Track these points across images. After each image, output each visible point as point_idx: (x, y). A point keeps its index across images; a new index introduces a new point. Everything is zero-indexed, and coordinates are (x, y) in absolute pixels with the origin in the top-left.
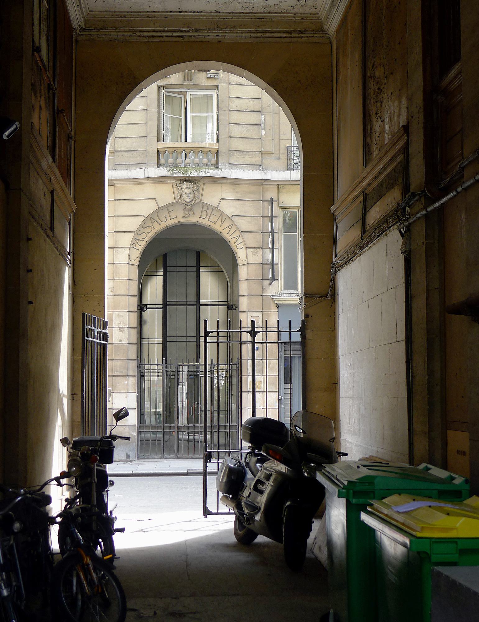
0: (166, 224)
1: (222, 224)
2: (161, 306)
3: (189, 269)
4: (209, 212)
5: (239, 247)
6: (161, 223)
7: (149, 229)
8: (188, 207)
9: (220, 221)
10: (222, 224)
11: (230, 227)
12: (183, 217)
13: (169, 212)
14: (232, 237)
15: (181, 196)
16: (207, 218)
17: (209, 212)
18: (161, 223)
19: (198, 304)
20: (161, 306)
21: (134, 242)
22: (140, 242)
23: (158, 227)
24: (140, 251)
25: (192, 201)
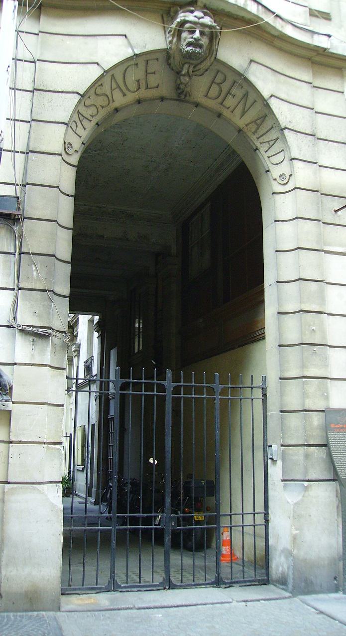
5: (276, 159)
9: (240, 107)
10: (244, 113)
11: (259, 122)
14: (261, 140)
21: (76, 118)
22: (85, 122)
24: (82, 139)
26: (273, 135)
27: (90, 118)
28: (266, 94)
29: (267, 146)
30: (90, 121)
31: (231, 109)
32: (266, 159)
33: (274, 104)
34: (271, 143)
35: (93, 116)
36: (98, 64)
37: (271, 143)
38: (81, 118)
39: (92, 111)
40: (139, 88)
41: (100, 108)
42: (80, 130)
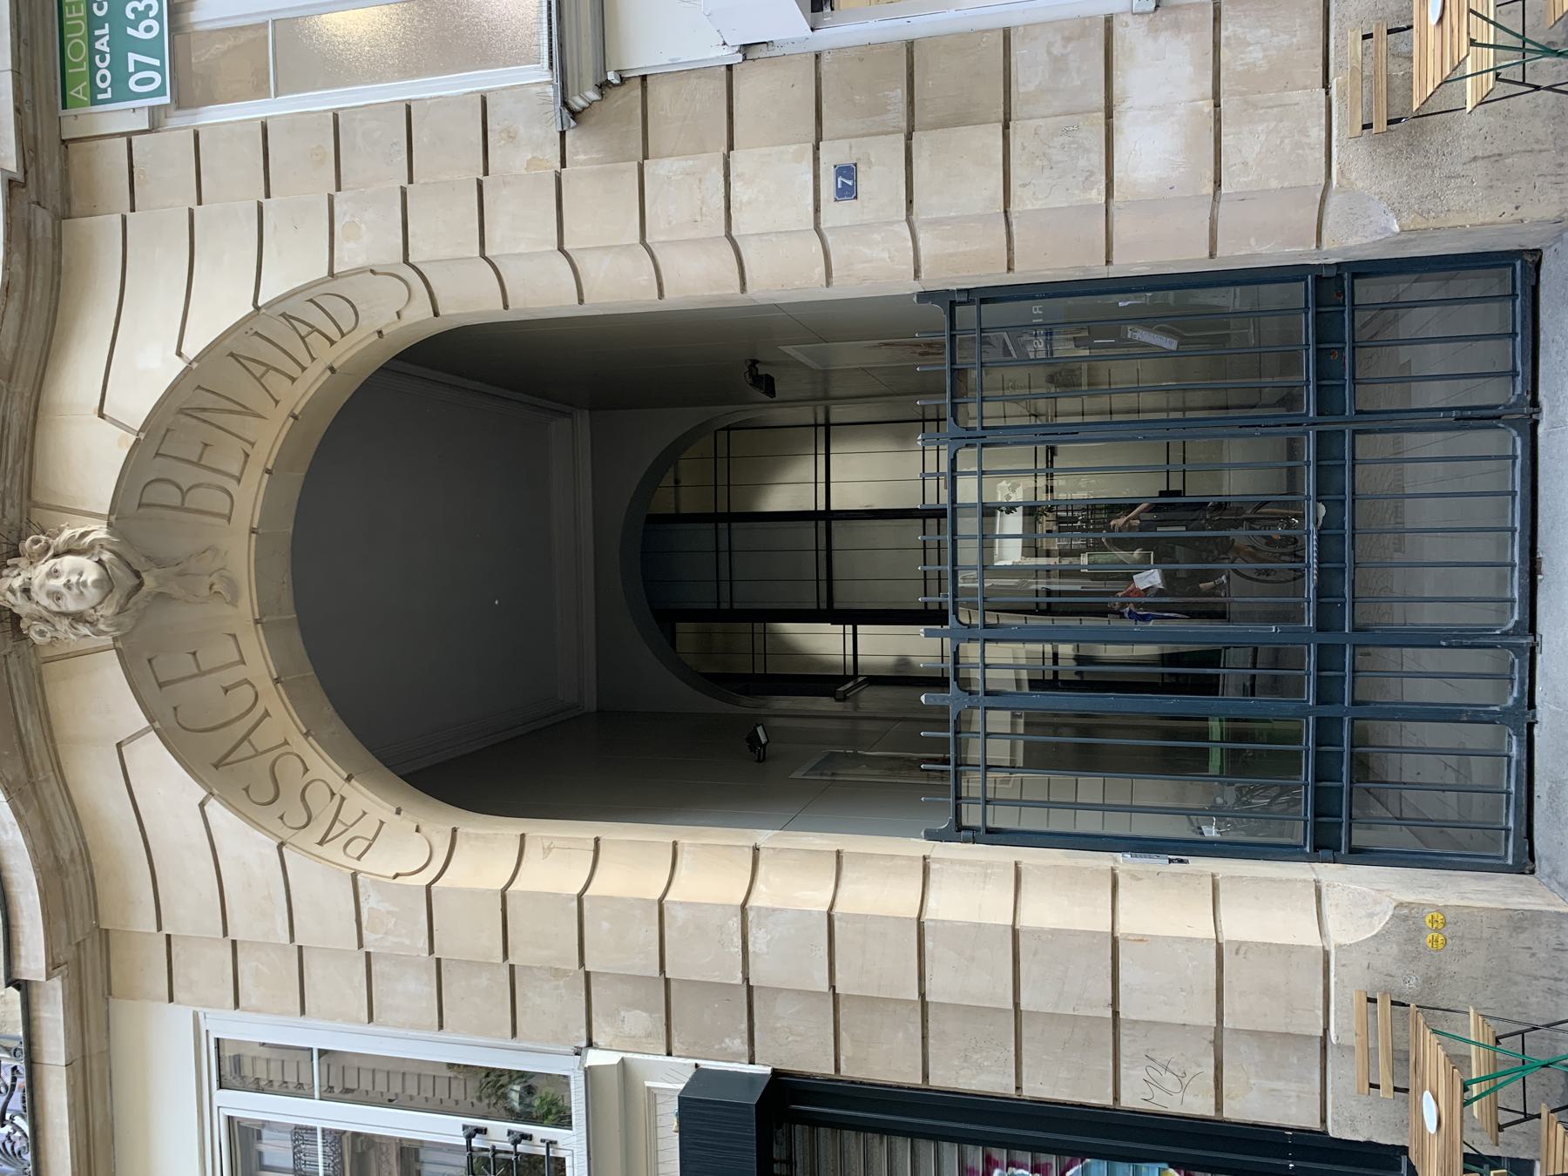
0: (266, 685)
1: (246, 411)
2: (849, 628)
3: (724, 545)
4: (187, 475)
6: (258, 712)
7: (290, 771)
8: (149, 582)
9: (232, 422)
10: (246, 411)
12: (233, 602)
13: (202, 674)
15: (77, 618)
16: (231, 485)
17: (187, 475)
18: (258, 712)
19: (828, 516)
20: (849, 628)
22: (347, 815)
23: (282, 722)
25: (100, 562)
26: (280, 331)
27: (337, 799)
28: (180, 365)
29: (314, 339)
30: (343, 799)
31: (248, 448)
32: (342, 345)
33: (192, 348)
34: (304, 330)
35: (333, 794)
36: (202, 805)
37: (304, 330)
38: (338, 828)
39: (317, 796)
40: (247, 682)
41: (309, 777)
42: (366, 828)
